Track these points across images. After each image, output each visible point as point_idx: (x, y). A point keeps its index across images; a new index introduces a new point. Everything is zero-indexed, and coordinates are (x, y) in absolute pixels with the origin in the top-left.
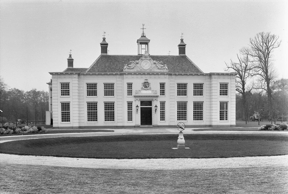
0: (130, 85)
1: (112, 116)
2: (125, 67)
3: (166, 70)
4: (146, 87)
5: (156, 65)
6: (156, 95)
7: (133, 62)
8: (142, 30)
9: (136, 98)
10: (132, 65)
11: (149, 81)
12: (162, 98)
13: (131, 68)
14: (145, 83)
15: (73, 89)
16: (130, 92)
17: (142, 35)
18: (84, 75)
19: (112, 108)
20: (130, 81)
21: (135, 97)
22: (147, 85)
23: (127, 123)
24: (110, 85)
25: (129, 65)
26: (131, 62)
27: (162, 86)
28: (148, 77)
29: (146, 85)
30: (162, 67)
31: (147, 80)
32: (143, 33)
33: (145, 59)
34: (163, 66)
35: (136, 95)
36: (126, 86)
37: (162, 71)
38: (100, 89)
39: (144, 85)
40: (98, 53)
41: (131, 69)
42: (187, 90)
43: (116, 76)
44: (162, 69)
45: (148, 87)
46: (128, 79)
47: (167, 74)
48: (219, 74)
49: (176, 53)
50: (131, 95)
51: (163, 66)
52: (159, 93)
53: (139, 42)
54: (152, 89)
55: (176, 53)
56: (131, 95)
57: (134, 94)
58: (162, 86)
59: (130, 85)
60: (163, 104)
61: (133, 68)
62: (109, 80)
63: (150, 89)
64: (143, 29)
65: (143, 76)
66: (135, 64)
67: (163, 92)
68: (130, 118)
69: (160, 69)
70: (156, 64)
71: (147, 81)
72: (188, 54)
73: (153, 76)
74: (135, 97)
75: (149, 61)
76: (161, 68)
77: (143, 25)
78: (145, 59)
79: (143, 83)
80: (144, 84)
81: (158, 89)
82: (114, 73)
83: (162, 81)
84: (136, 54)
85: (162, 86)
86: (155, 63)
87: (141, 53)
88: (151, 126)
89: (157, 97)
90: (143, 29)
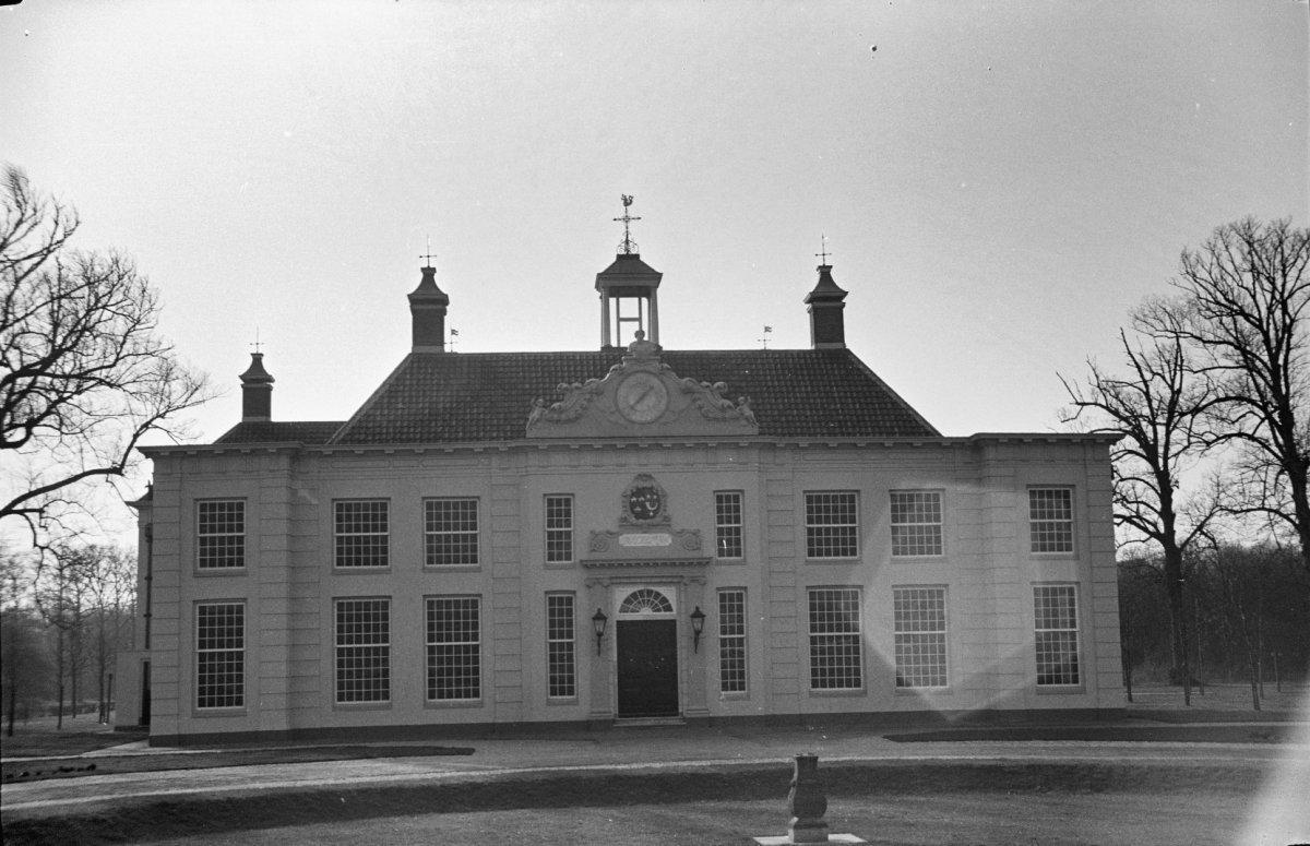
0: (559, 509)
1: (350, 674)
2: (535, 414)
3: (744, 422)
4: (643, 515)
5: (694, 400)
6: (696, 554)
7: (577, 388)
8: (622, 224)
9: (597, 574)
10: (571, 403)
11: (664, 482)
12: (728, 575)
13: (563, 416)
14: (639, 492)
15: (264, 532)
16: (558, 547)
17: (624, 253)
18: (320, 455)
19: (376, 628)
20: (558, 486)
21: (587, 566)
22: (648, 504)
23: (327, 712)
24: (447, 505)
25: (556, 405)
26: (565, 385)
27: (728, 505)
28: (653, 463)
29: (644, 506)
30: (723, 409)
31: (649, 477)
32: (627, 242)
34: (729, 407)
35: (596, 556)
36: (538, 515)
38: (407, 534)
39: (633, 505)
40: (397, 345)
42: (744, 527)
44: (724, 419)
45: (656, 512)
46: (558, 475)
47: (751, 446)
48: (185, 453)
49: (797, 336)
50: (568, 557)
51: (727, 402)
52: (710, 550)
55: (797, 336)
56: (568, 557)
57: (580, 550)
58: (728, 509)
59: (559, 509)
60: (732, 602)
62: (451, 479)
63: (666, 525)
64: (627, 219)
65: (632, 459)
66: (588, 396)
67: (732, 543)
68: (562, 684)
70: (697, 396)
71: (647, 484)
72: (858, 340)
73: (678, 458)
74: (586, 566)
75: (655, 382)
76: (720, 415)
77: (627, 202)
78: (636, 368)
79: (629, 493)
80: (634, 499)
81: (707, 523)
82: (478, 446)
83: (728, 483)
84: (594, 345)
85: (728, 505)
86: (687, 391)
87: (619, 341)
88: (672, 721)
89: (704, 563)
90: (627, 219)
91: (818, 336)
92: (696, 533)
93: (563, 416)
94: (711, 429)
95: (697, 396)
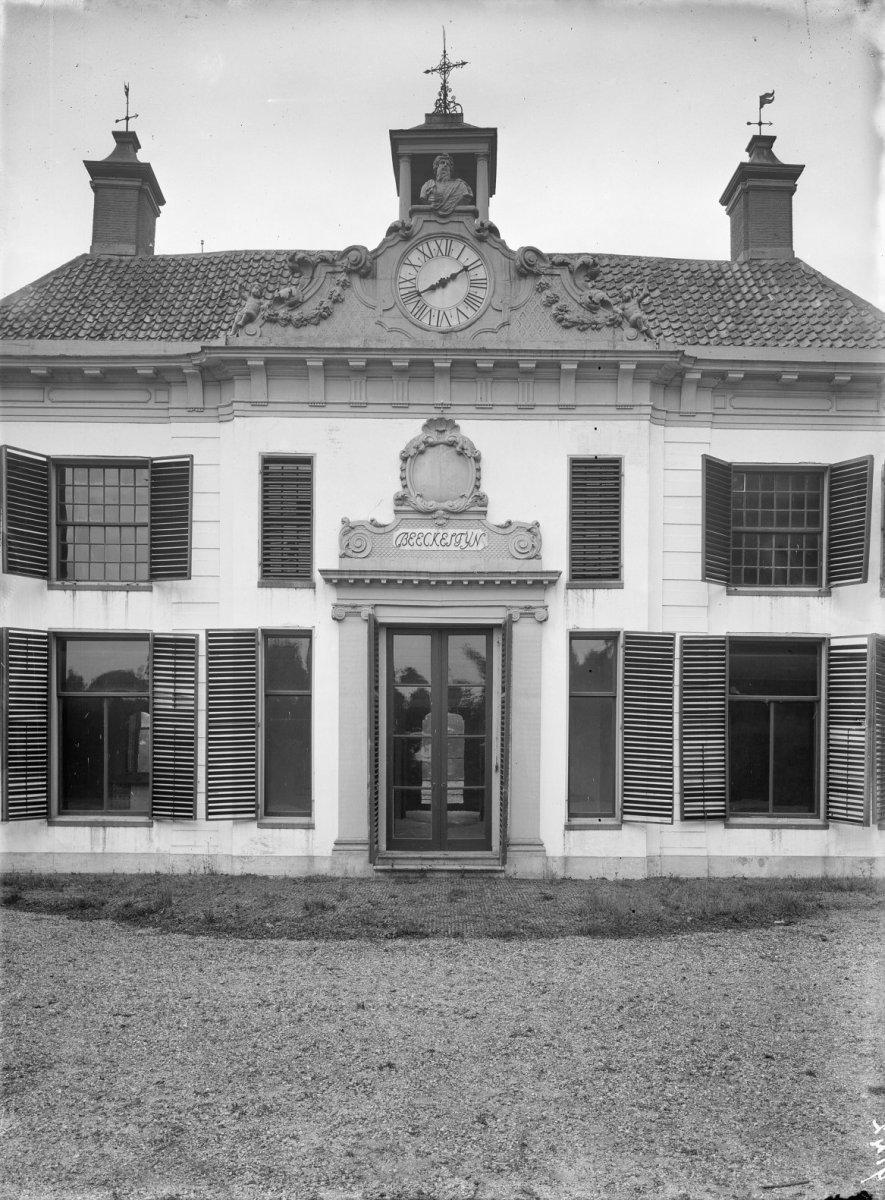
5: (541, 289)
6: (532, 566)
8: (436, 79)
13: (296, 315)
30: (593, 306)
33: (433, 228)
37: (599, 341)
41: (303, 323)
43: (162, 396)
52: (556, 556)
53: (403, 149)
54: (490, 509)
61: (324, 316)
64: (445, 68)
65: (419, 393)
66: (342, 277)
69: (582, 326)
76: (587, 317)
89: (543, 582)
91: (741, 238)
92: (533, 530)
93: (296, 315)
94: (573, 340)
95: (543, 279)
